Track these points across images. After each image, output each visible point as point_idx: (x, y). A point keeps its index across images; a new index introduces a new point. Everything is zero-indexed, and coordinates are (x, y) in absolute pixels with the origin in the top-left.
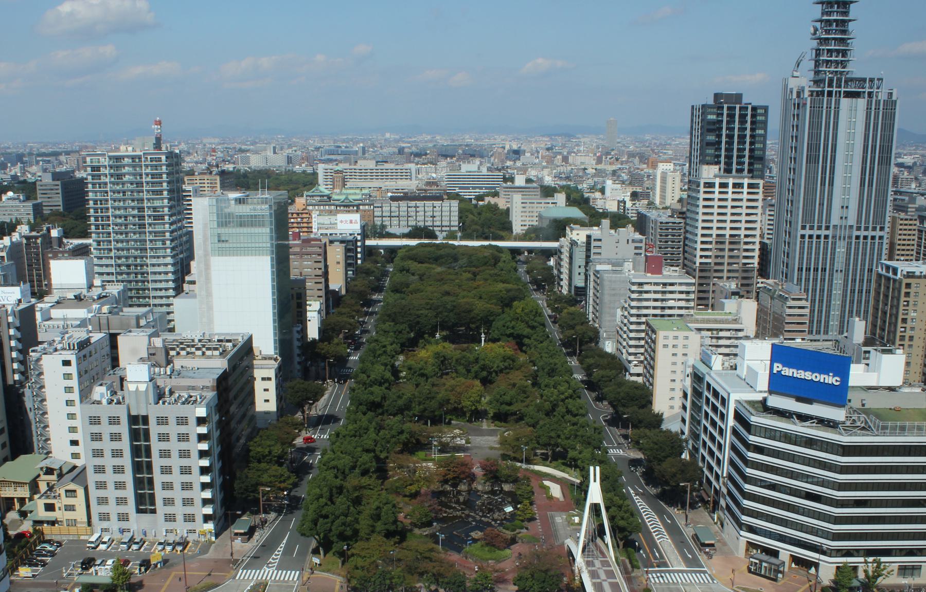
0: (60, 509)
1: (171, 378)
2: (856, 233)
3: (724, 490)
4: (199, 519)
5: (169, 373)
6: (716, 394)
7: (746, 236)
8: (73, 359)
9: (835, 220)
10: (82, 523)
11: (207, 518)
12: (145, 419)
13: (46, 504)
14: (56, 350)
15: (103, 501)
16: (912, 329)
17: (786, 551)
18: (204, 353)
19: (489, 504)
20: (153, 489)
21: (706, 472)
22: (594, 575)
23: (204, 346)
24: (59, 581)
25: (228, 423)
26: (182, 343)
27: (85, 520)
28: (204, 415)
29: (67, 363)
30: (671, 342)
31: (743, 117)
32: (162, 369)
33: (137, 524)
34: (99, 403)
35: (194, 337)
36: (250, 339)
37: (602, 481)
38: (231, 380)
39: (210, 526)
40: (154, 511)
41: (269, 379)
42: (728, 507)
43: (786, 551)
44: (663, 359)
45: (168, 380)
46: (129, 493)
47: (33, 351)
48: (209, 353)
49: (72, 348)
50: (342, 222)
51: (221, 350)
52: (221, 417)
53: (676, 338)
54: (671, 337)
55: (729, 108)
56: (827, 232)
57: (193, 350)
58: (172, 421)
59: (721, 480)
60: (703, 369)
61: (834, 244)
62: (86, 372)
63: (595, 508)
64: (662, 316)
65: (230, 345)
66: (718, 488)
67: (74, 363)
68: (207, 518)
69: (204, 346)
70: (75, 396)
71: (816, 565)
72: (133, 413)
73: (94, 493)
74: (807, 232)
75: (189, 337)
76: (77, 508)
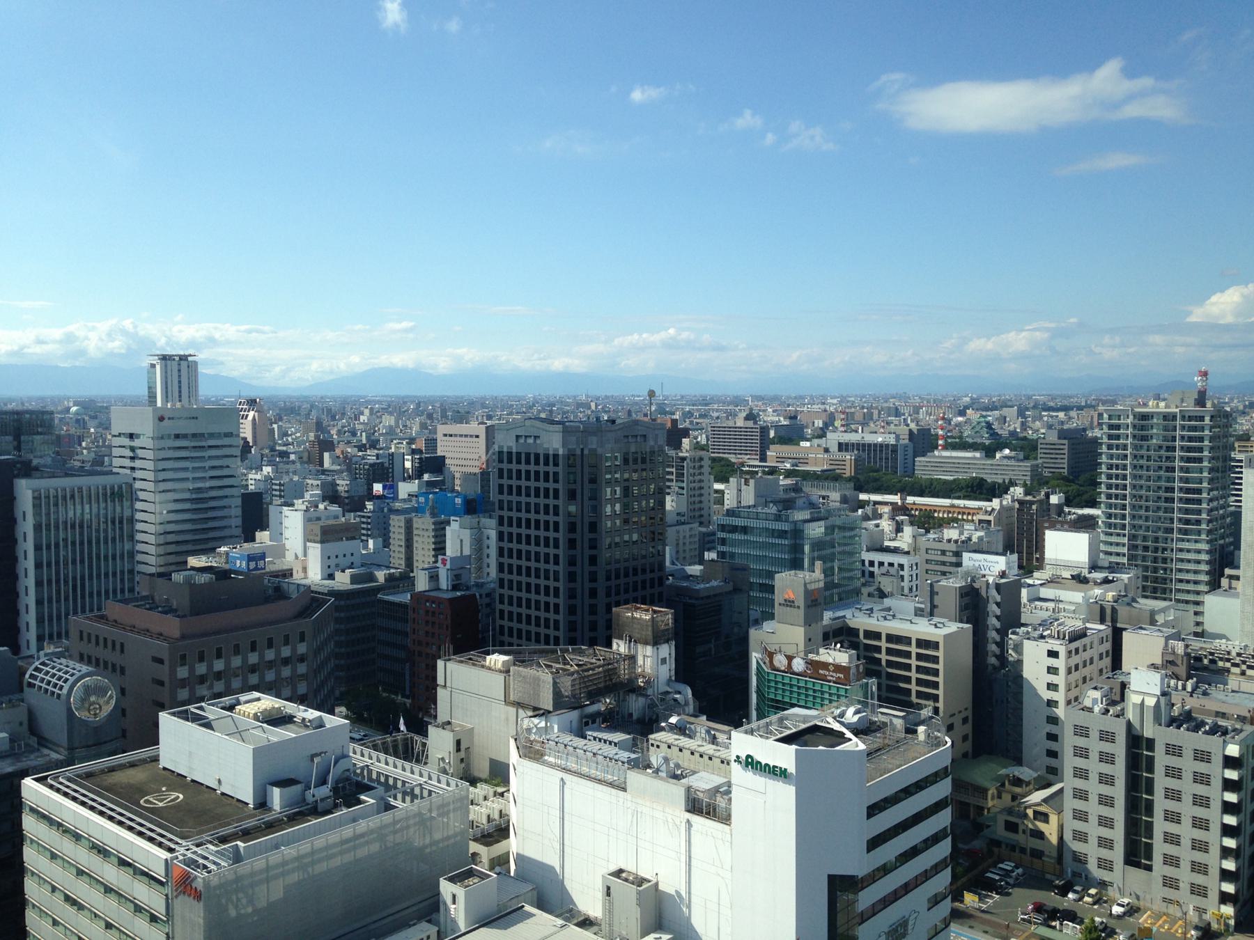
1: (1191, 696)
5: (1189, 689)
8: (1062, 651)
10: (1048, 856)
12: (1150, 744)
13: (1006, 822)
18: (1243, 673)
23: (1244, 662)
24: (1011, 924)
26: (1212, 654)
27: (1055, 854)
29: (1053, 654)
32: (1180, 683)
34: (1090, 710)
35: (1230, 648)
40: (1149, 868)
46: (1118, 834)
47: (1014, 633)
49: (1061, 637)
57: (1228, 665)
58: (1188, 753)
62: (1077, 668)
67: (1062, 654)
69: (1244, 662)
75: (1223, 647)
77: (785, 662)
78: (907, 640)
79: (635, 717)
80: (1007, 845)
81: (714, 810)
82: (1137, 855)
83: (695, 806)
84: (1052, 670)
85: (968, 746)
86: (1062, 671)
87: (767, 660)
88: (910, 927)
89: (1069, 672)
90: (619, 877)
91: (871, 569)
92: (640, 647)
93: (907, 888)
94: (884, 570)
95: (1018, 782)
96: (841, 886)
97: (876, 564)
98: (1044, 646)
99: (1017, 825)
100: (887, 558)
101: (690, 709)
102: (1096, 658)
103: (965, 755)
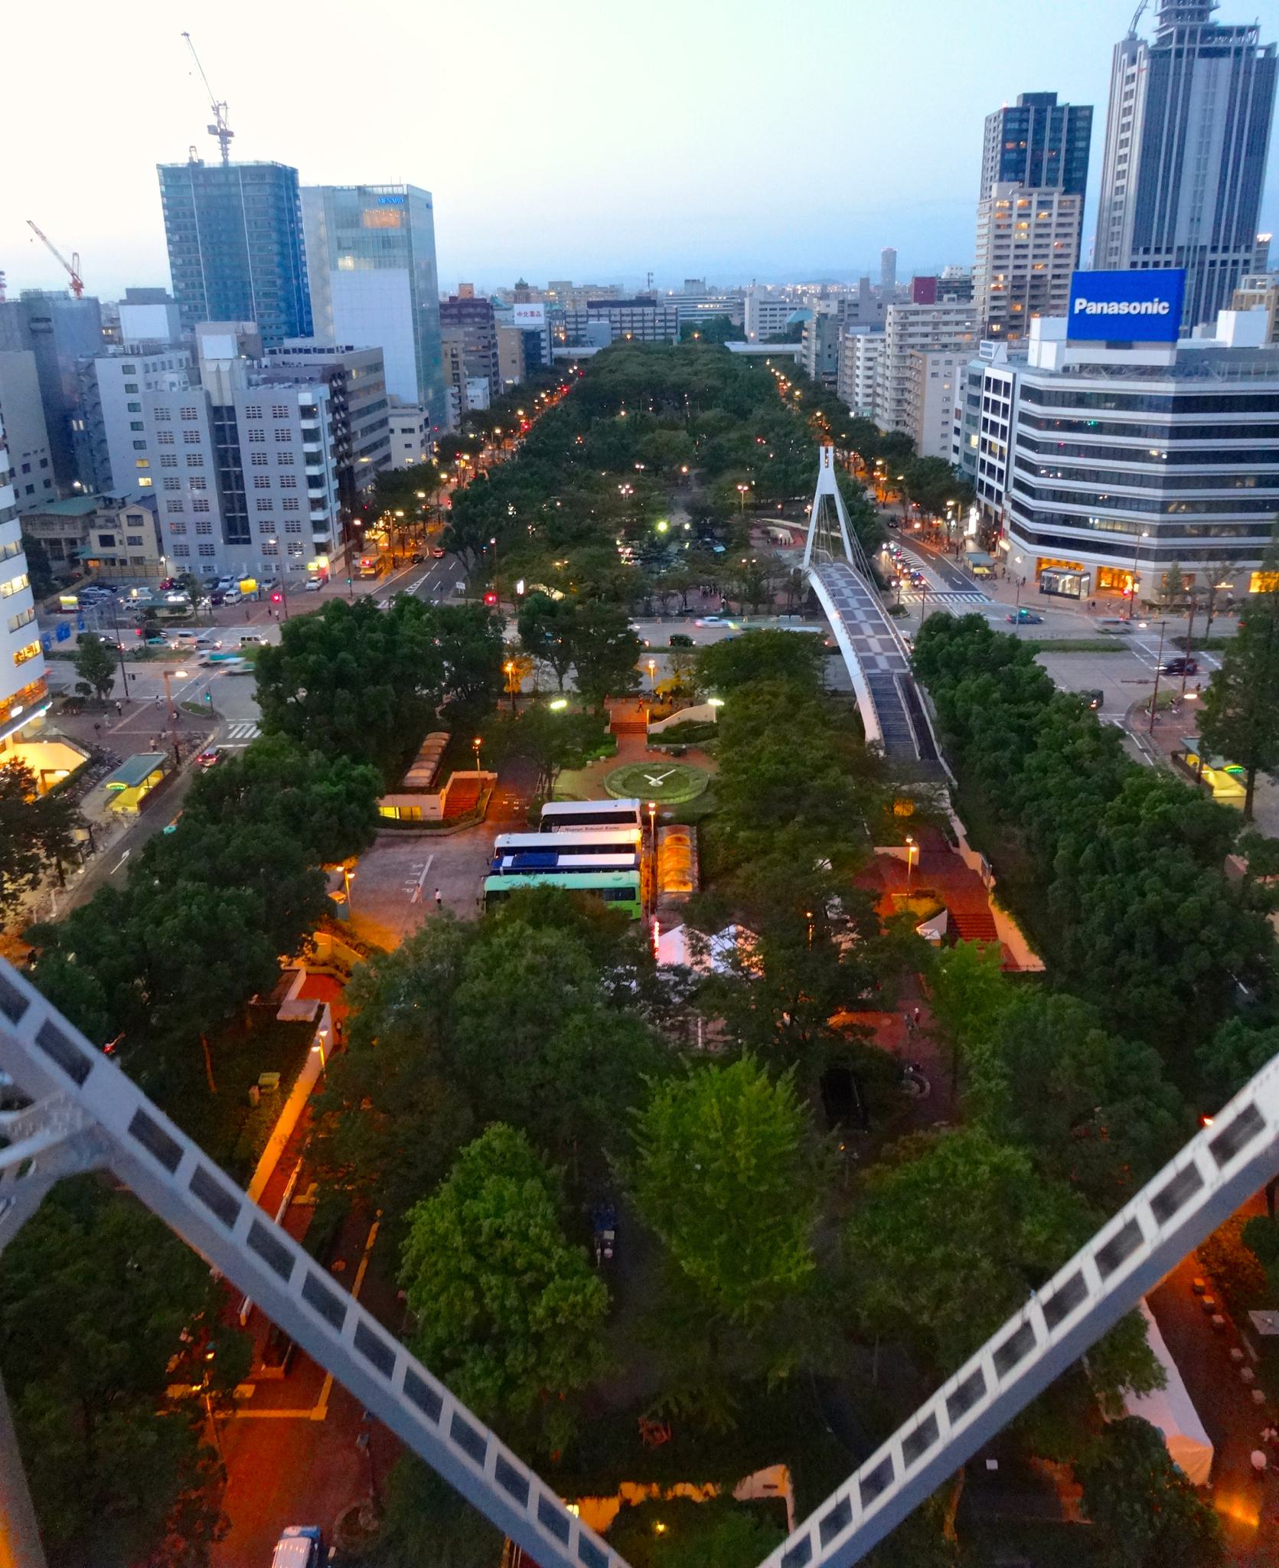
0: (121, 542)
2: (1210, 256)
7: (1055, 277)
9: (1181, 239)
12: (231, 410)
30: (941, 369)
31: (1056, 129)
40: (248, 541)
41: (411, 431)
46: (214, 515)
50: (520, 314)
53: (949, 362)
55: (1036, 111)
63: (829, 500)
67: (139, 368)
72: (216, 402)
73: (167, 518)
82: (236, 530)
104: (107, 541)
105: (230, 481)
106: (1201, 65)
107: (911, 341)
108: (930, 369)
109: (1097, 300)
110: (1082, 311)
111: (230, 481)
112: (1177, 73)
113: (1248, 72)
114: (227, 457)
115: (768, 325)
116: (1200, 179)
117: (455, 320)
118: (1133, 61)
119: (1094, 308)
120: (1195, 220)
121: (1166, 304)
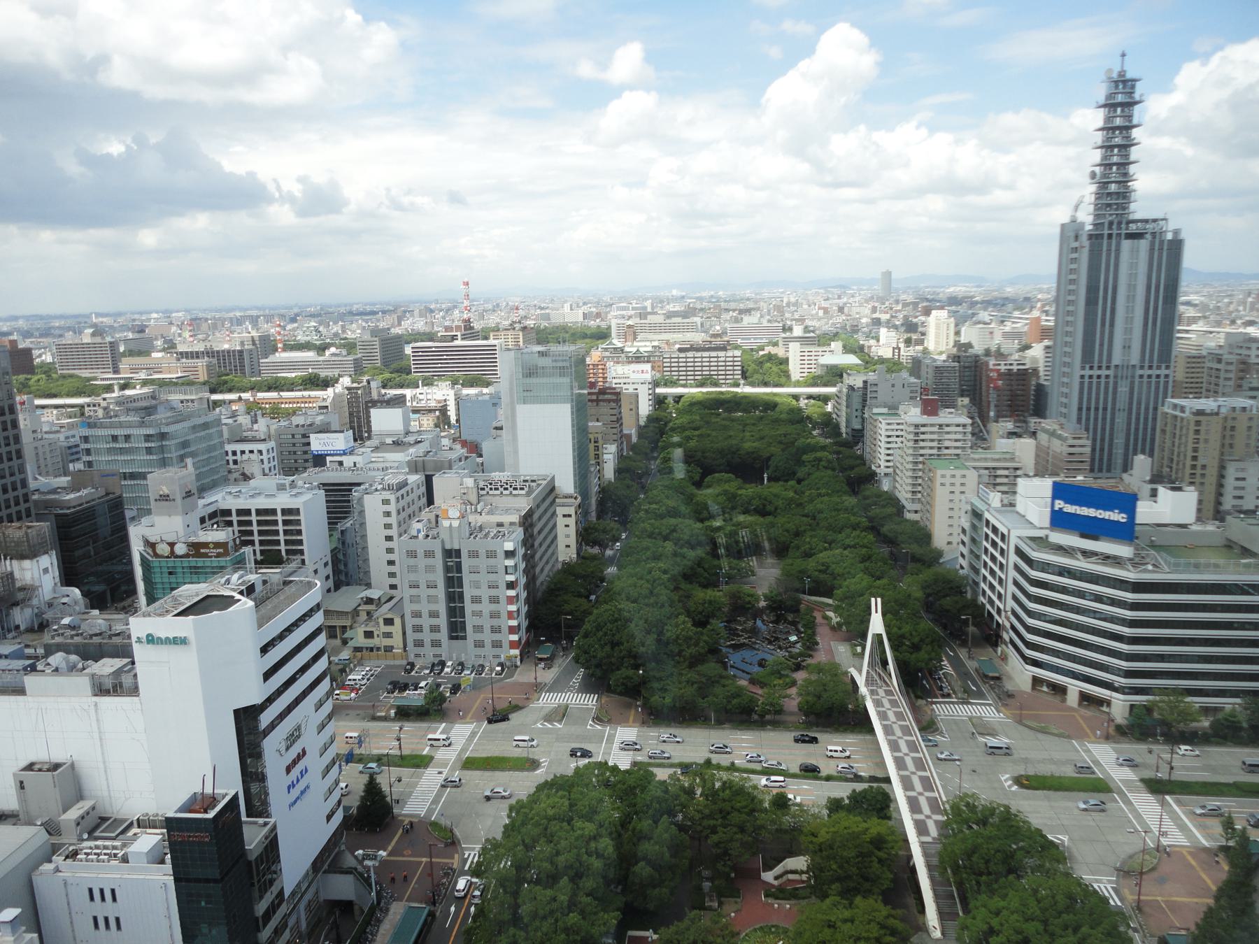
3: (1008, 625)
4: (506, 645)
6: (995, 530)
8: (392, 498)
9: (1117, 359)
11: (513, 645)
12: (458, 553)
14: (376, 490)
15: (418, 629)
16: (1204, 467)
17: (1075, 687)
18: (511, 493)
19: (774, 632)
20: (464, 617)
21: (988, 606)
22: (878, 703)
25: (533, 556)
26: (491, 484)
28: (512, 549)
29: (386, 502)
33: (451, 652)
36: (554, 477)
37: (884, 614)
38: (536, 516)
39: (516, 652)
40: (464, 638)
41: (570, 516)
42: (1012, 642)
43: (1075, 687)
44: (941, 496)
45: (478, 516)
46: (443, 621)
48: (514, 492)
51: (526, 489)
52: (527, 550)
53: (953, 476)
54: (948, 476)
56: (1107, 372)
59: (1003, 613)
60: (980, 506)
61: (1116, 383)
64: (938, 455)
65: (534, 484)
66: (1000, 621)
68: (513, 645)
70: (393, 532)
71: (1109, 703)
72: (448, 547)
73: (410, 622)
74: (1087, 372)
76: (394, 634)
77: (168, 549)
78: (273, 512)
79: (22, 628)
80: (367, 648)
81: (121, 686)
82: (457, 629)
83: (101, 690)
84: (388, 514)
85: (331, 583)
86: (394, 514)
87: (150, 551)
88: (303, 729)
89: (399, 513)
90: (32, 770)
91: (235, 458)
92: (15, 562)
93: (297, 701)
94: (245, 457)
95: (369, 601)
96: (246, 719)
97: (238, 453)
98: (378, 497)
99: (372, 632)
100: (247, 447)
101: (81, 606)
102: (416, 499)
103: (329, 591)
104: (369, 635)
105: (455, 597)
106: (1126, 244)
107: (922, 452)
108: (939, 480)
109: (1072, 504)
110: (1061, 509)
111: (455, 597)
112: (1109, 250)
113: (1161, 249)
114: (454, 582)
115: (806, 362)
116: (1129, 320)
117: (595, 404)
118: (1077, 238)
119: (1070, 509)
120: (1127, 347)
121: (1124, 516)
